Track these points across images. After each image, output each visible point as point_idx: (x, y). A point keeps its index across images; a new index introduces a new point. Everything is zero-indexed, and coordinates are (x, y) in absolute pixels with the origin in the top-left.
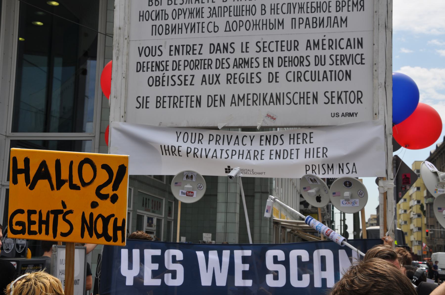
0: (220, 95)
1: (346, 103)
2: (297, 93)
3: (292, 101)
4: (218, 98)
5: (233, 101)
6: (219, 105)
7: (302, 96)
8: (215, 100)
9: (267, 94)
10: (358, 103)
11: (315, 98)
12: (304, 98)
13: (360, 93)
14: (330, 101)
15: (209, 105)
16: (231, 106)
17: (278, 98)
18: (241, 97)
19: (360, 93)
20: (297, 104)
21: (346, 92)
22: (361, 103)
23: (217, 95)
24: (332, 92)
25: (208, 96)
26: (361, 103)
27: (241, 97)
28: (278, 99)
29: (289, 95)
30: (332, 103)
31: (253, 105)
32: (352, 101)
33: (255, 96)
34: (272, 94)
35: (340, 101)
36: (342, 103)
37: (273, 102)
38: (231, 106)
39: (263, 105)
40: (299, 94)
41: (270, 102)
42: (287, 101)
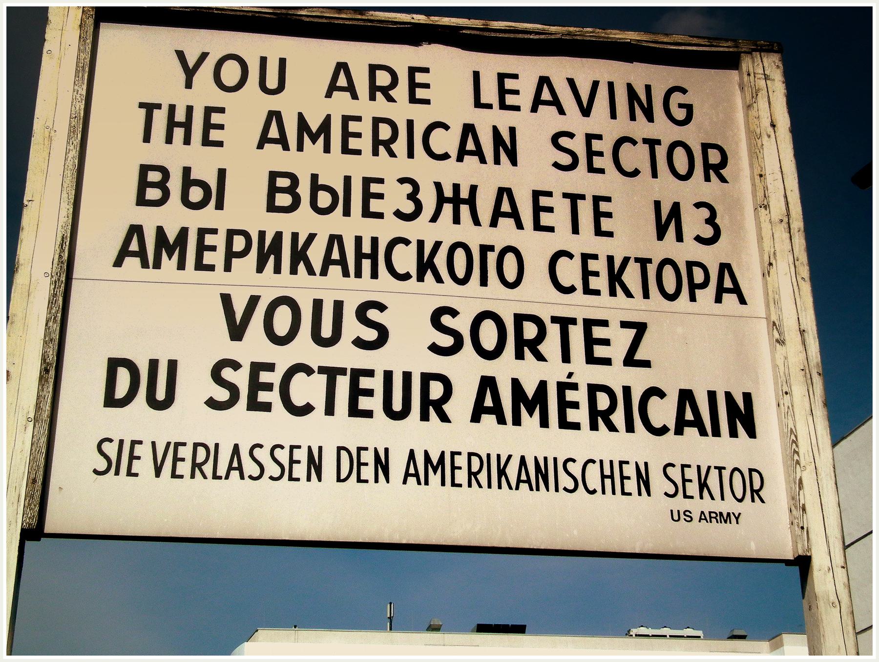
0: (376, 450)
1: (723, 499)
2: (593, 462)
3: (580, 483)
4: (368, 457)
5: (412, 470)
6: (371, 478)
7: (607, 472)
8: (360, 464)
9: (510, 457)
10: (753, 501)
11: (644, 481)
12: (612, 477)
13: (755, 476)
14: (679, 490)
15: (343, 476)
16: (405, 482)
17: (542, 473)
18: (435, 461)
19: (755, 474)
20: (594, 492)
21: (720, 469)
22: (763, 501)
23: (366, 449)
24: (683, 466)
25: (339, 449)
26: (763, 501)
27: (435, 461)
28: (539, 475)
29: (570, 465)
30: (685, 496)
31: (470, 485)
32: (739, 496)
33: (475, 461)
34: (523, 458)
35: (705, 491)
36: (713, 498)
37: (528, 481)
38: (405, 482)
39: (500, 487)
40: (598, 464)
41: (519, 481)
42: (566, 481)
